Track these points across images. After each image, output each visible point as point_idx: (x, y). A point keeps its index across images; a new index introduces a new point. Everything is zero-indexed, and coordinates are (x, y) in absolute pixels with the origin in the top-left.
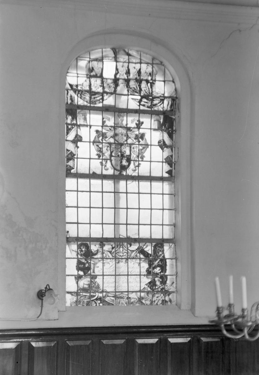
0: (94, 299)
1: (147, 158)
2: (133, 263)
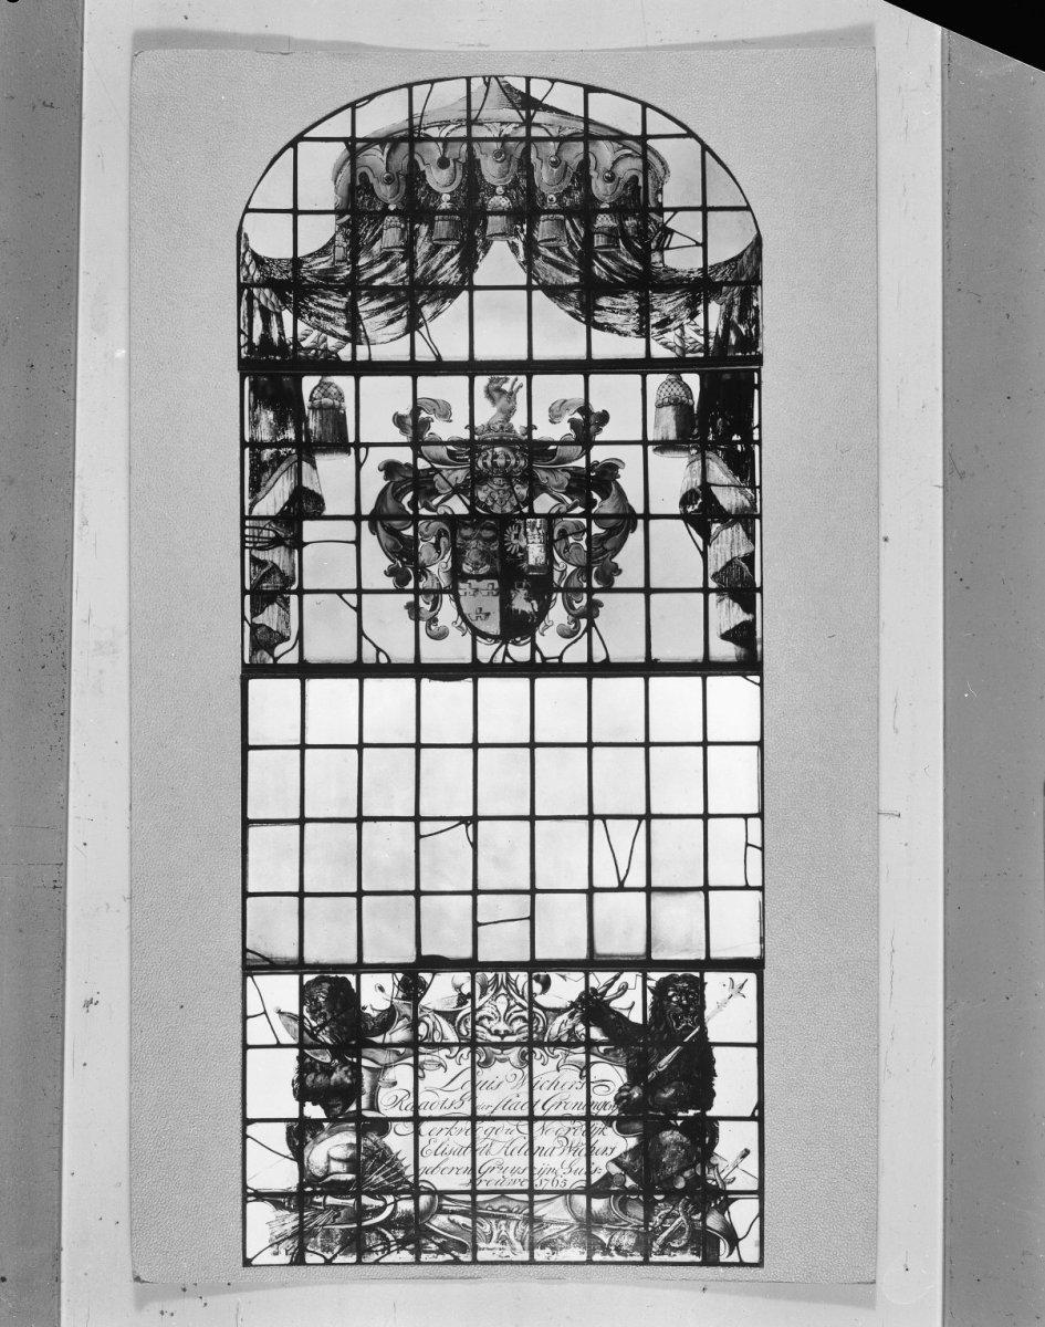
0: (380, 1224)
1: (631, 575)
2: (553, 1063)
